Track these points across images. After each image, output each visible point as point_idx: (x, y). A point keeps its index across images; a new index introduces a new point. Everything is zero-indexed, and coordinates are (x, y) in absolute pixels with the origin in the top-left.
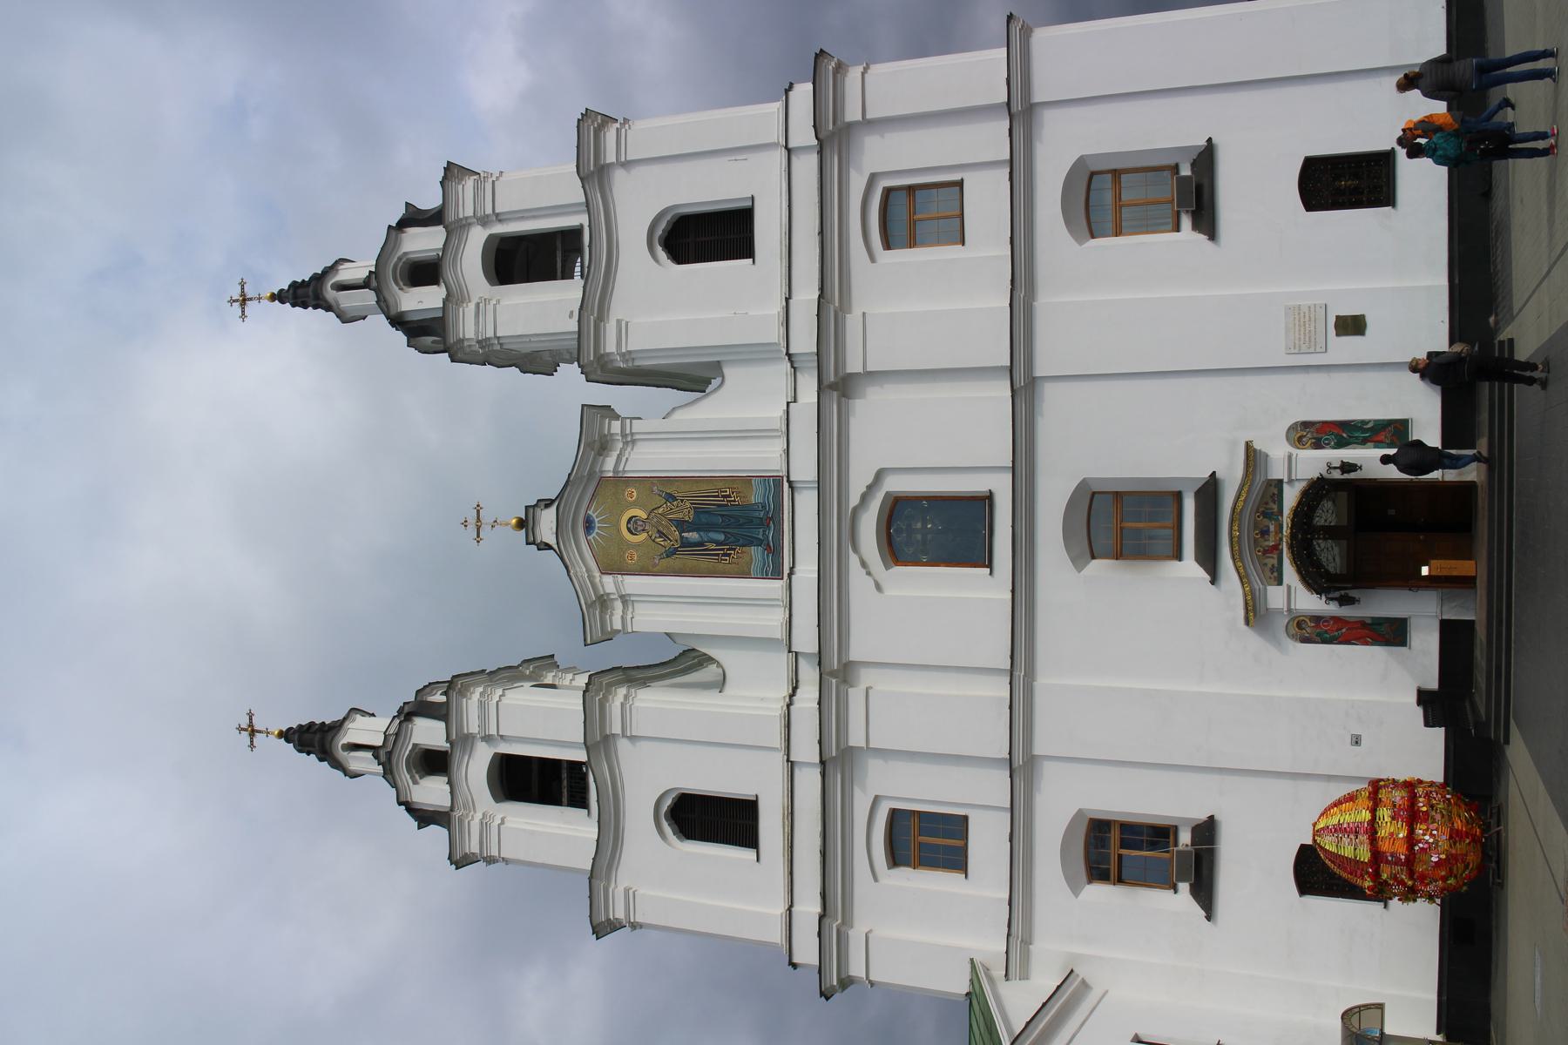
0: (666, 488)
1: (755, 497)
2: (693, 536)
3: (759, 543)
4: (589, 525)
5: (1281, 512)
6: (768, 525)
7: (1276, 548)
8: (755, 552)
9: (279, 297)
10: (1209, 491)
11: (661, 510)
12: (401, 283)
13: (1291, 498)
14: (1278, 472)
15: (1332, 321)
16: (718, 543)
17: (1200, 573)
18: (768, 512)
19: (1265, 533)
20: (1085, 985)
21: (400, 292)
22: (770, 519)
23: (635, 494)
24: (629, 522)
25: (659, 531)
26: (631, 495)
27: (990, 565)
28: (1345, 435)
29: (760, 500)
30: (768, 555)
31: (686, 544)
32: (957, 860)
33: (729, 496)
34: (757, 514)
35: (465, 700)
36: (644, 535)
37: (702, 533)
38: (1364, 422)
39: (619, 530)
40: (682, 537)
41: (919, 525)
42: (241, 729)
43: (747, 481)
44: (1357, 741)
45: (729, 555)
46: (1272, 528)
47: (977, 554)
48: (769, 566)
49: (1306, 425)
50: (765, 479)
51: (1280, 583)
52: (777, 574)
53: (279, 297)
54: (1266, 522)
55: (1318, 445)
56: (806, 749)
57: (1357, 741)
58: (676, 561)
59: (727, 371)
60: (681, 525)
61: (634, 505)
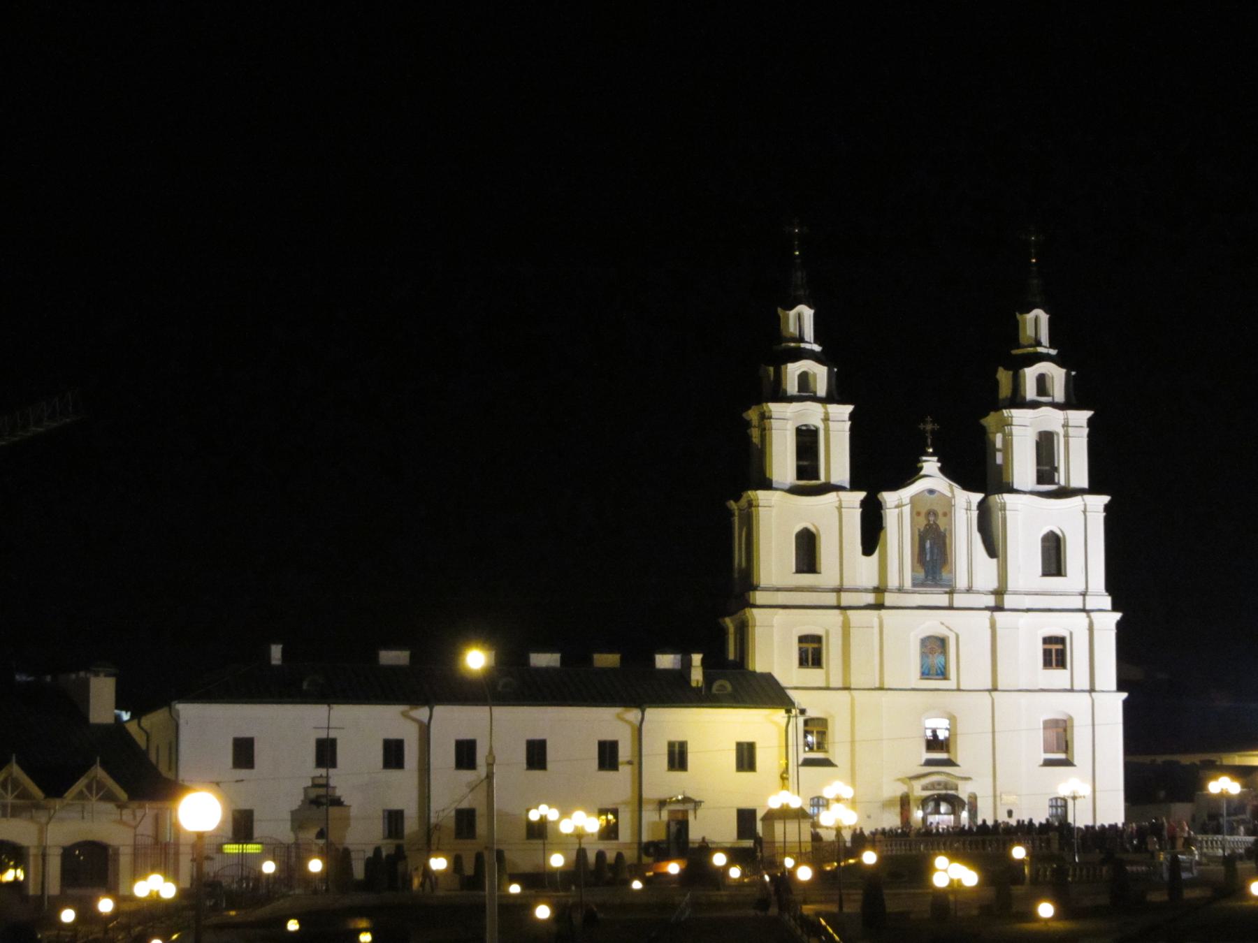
1: (945, 575)
2: (928, 545)
3: (926, 577)
8: (921, 574)
15: (1012, 808)
22: (936, 583)
29: (944, 578)
32: (803, 662)
43: (951, 572)
46: (941, 787)
47: (926, 674)
52: (914, 585)
54: (943, 784)
56: (847, 599)
57: (869, 817)
58: (917, 538)
59: (995, 561)
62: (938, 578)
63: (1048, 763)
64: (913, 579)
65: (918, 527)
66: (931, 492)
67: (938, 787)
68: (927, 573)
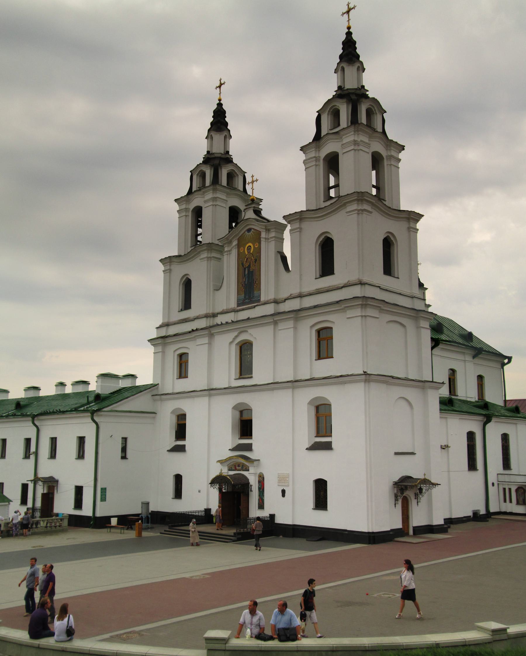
0: (257, 260)
2: (247, 273)
3: (245, 297)
4: (249, 230)
5: (243, 470)
6: (249, 299)
7: (236, 469)
9: (349, 34)
10: (249, 448)
11: (253, 258)
12: (331, 110)
13: (245, 473)
14: (252, 470)
16: (245, 282)
17: (235, 446)
18: (252, 299)
19: (239, 466)
20: (154, 418)
21: (327, 112)
22: (251, 300)
23: (257, 247)
24: (250, 246)
25: (248, 258)
26: (256, 245)
27: (239, 378)
28: (261, 490)
30: (242, 301)
31: (245, 269)
33: (256, 283)
34: (252, 295)
35: (212, 191)
36: (247, 253)
37: (247, 275)
38: (264, 496)
39: (248, 243)
40: (246, 268)
41: (249, 353)
42: (220, 80)
43: (260, 289)
44: (199, 491)
45: (242, 287)
46: (240, 468)
48: (240, 301)
49: (263, 478)
50: (260, 296)
51: (229, 470)
52: (239, 305)
53: (349, 34)
54: (241, 466)
55: (259, 482)
60: (249, 267)
61: (254, 247)
62: (252, 297)
63: (315, 447)
64: (238, 300)
65: (241, 260)
66: (249, 230)
67: (238, 468)
68: (245, 294)
